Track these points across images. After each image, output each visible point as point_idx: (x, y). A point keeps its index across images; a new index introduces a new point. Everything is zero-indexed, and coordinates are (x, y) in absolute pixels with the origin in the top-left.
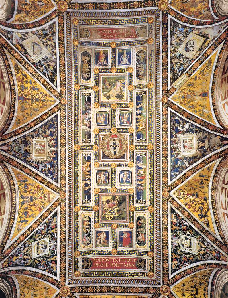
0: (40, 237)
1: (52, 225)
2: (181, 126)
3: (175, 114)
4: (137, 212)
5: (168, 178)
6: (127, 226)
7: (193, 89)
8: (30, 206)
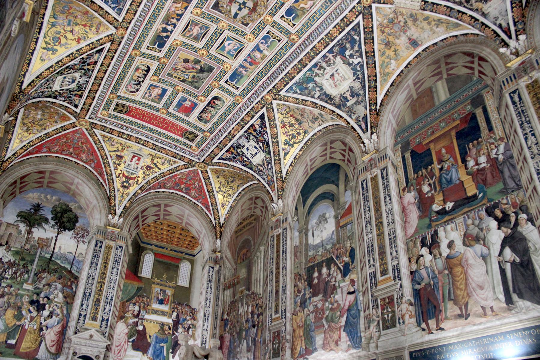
0: (69, 72)
1: (90, 61)
2: (351, 52)
3: (360, 31)
4: (219, 91)
5: (284, 87)
6: (197, 97)
7: (410, 25)
8: (65, 31)
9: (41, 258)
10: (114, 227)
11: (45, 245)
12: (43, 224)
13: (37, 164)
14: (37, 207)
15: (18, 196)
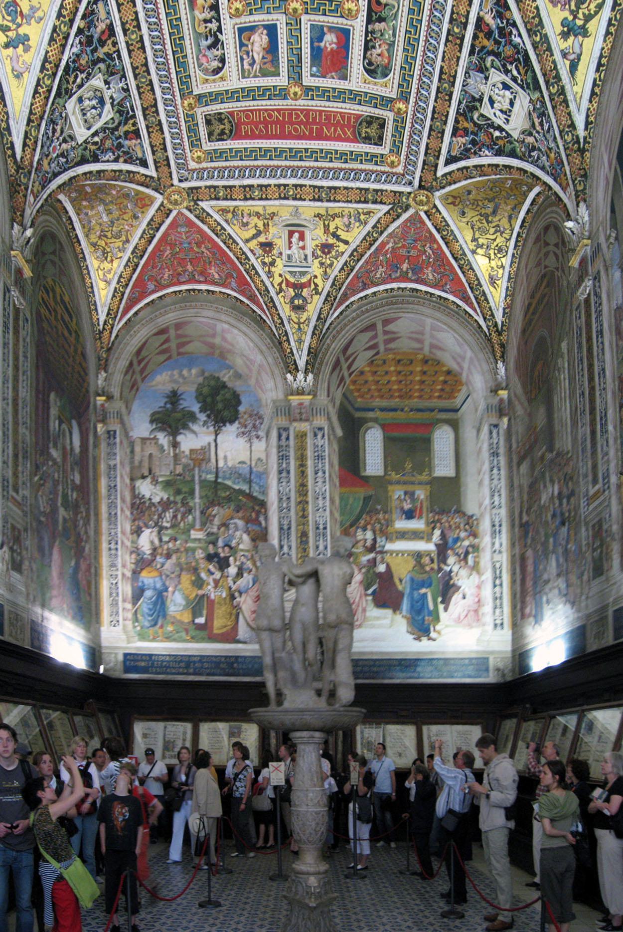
9: (203, 482)
10: (298, 394)
11: (202, 460)
12: (190, 425)
13: (152, 320)
14: (174, 397)
15: (142, 386)
